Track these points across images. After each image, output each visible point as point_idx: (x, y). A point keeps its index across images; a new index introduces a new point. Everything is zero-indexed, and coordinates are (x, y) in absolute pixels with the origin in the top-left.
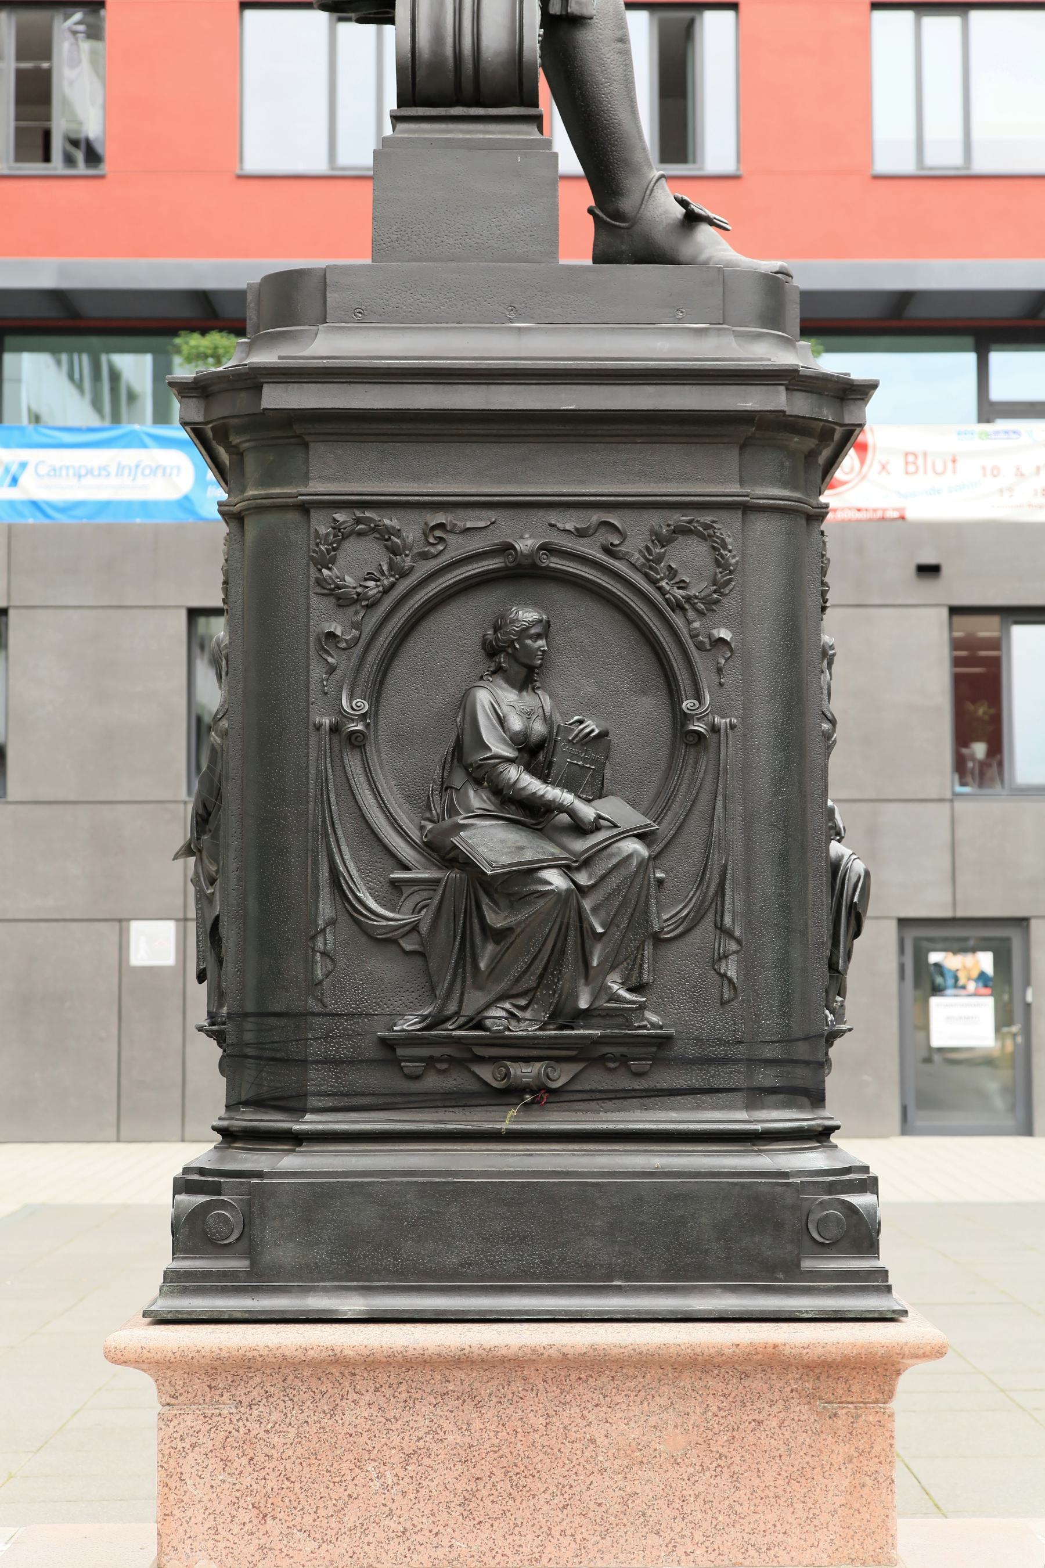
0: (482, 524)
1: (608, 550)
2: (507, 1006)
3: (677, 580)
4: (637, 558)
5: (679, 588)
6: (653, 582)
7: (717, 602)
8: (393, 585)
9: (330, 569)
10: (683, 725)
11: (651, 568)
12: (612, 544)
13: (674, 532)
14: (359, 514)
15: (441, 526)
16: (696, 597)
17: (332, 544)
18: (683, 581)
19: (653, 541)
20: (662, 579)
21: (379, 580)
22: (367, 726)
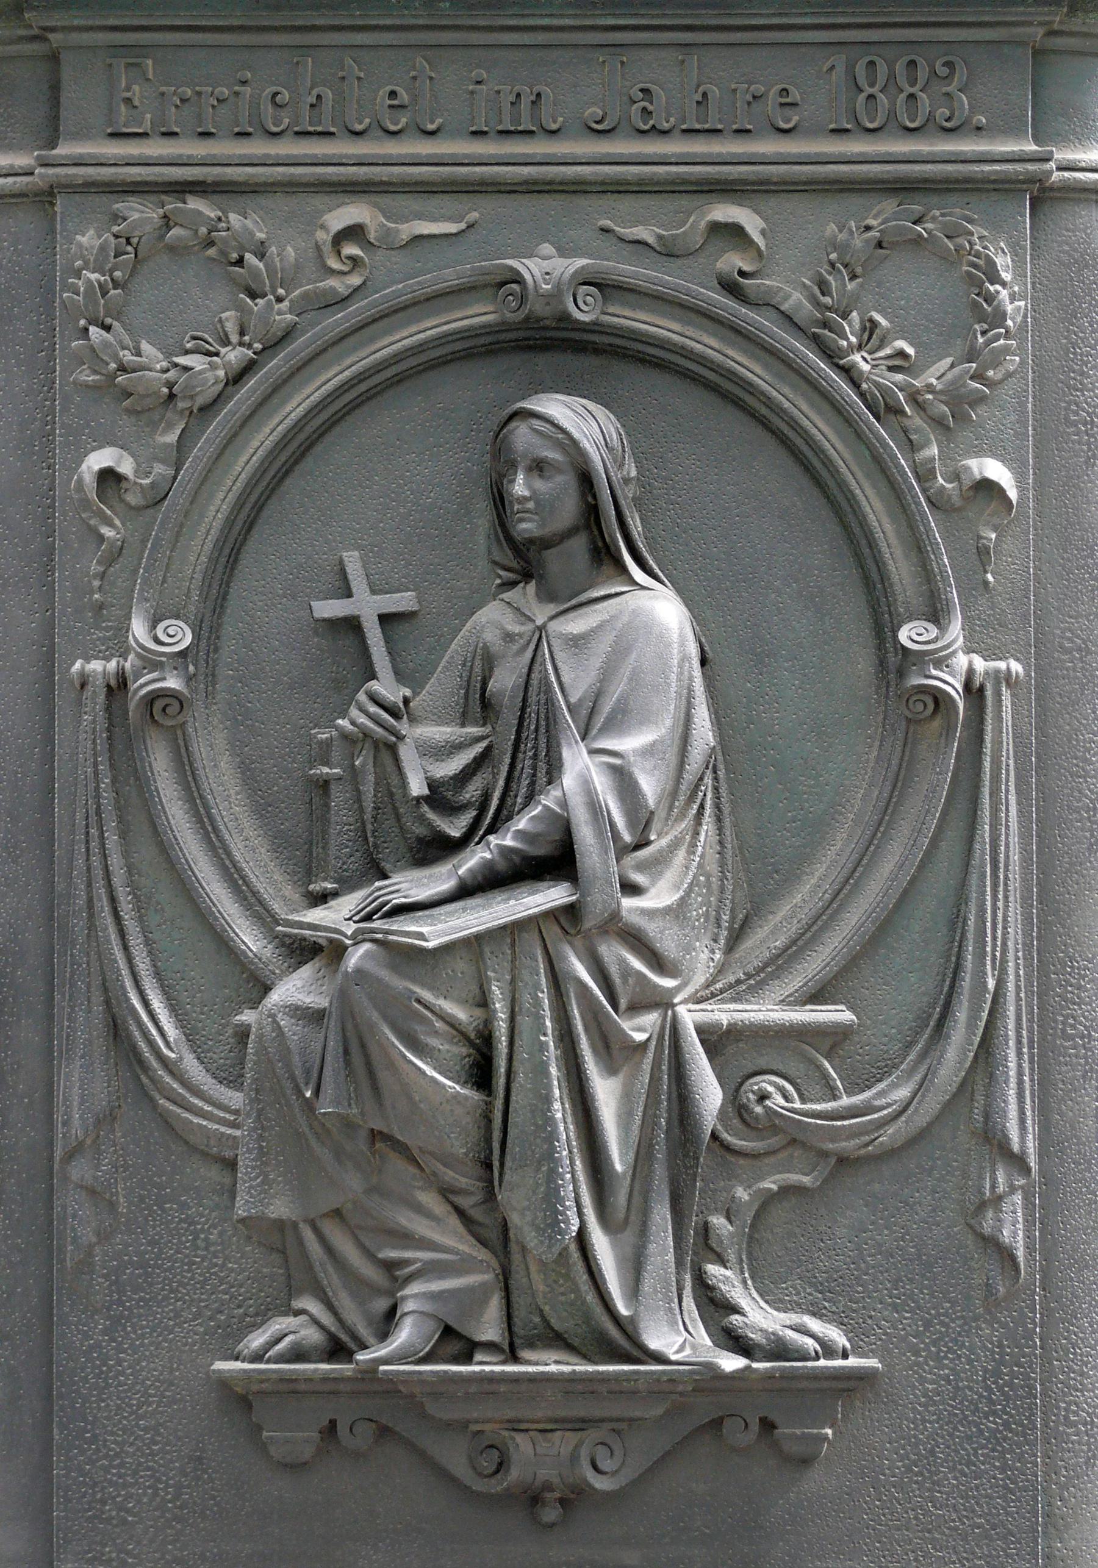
0: (452, 228)
1: (731, 287)
2: (676, 1338)
3: (888, 351)
4: (796, 300)
5: (891, 369)
6: (831, 355)
7: (979, 400)
8: (248, 369)
9: (108, 328)
10: (901, 673)
11: (825, 324)
12: (742, 273)
13: (880, 245)
14: (172, 205)
15: (354, 233)
16: (930, 388)
17: (111, 271)
18: (901, 354)
19: (832, 265)
20: (851, 348)
21: (217, 354)
22: (189, 679)
